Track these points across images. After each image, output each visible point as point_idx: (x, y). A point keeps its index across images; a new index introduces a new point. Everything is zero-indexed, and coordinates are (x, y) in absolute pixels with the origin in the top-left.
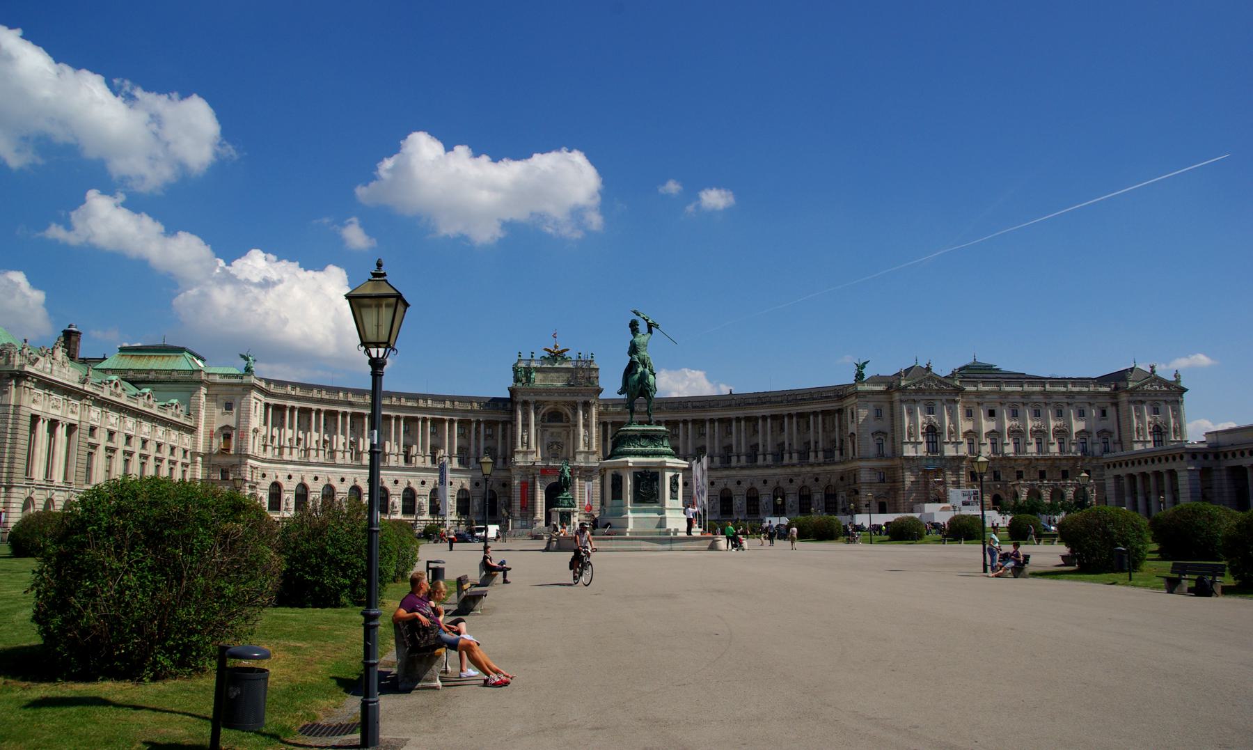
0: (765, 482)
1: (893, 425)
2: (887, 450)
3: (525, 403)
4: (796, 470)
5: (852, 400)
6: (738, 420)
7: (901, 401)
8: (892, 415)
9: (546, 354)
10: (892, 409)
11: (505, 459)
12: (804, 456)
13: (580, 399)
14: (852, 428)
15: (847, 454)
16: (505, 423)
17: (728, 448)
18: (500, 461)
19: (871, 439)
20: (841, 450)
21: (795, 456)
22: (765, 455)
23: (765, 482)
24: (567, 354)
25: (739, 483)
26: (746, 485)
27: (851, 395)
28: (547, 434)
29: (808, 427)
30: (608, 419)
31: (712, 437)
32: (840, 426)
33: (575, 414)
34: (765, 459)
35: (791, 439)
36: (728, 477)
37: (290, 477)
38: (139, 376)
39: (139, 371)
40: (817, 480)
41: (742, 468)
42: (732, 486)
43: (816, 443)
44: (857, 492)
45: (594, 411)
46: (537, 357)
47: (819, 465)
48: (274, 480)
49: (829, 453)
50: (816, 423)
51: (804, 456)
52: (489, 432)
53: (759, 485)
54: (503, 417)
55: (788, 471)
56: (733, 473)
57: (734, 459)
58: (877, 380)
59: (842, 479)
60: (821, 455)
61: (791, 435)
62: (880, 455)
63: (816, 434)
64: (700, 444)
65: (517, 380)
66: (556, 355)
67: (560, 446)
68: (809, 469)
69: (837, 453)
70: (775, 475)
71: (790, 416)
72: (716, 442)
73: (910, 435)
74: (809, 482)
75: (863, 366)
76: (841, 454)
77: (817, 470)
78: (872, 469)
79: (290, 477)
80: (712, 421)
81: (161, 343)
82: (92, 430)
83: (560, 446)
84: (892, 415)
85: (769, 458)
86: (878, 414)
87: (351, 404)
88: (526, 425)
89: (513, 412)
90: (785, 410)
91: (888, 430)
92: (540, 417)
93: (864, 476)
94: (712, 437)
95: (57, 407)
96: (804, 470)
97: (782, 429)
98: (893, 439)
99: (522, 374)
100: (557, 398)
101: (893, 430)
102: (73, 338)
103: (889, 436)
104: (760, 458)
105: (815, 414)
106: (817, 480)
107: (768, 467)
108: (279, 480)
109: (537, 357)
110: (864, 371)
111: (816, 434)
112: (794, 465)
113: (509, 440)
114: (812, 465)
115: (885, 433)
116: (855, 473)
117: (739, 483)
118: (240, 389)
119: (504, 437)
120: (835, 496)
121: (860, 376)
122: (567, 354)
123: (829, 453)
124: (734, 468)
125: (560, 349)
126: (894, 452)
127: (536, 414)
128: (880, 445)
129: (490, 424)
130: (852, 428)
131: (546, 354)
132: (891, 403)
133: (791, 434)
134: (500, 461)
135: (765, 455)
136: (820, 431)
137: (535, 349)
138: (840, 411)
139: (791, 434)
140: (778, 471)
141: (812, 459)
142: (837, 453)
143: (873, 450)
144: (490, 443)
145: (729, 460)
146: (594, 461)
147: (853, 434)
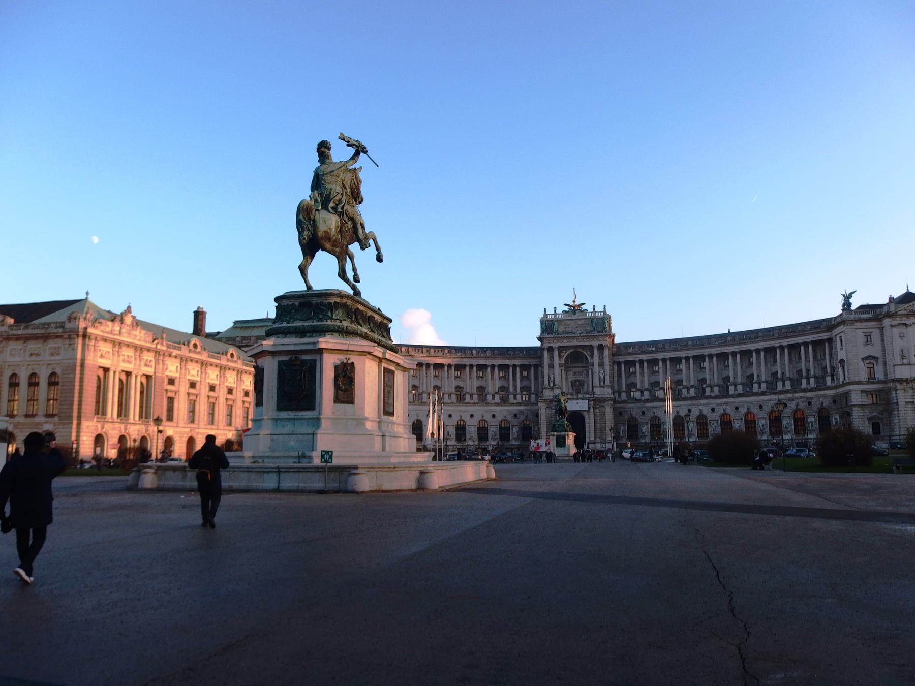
0: (761, 407)
1: (884, 349)
2: (879, 375)
3: (551, 349)
4: (790, 395)
5: (841, 328)
6: (734, 354)
7: (892, 326)
8: (883, 341)
9: (566, 308)
10: (882, 335)
11: (537, 395)
12: (796, 383)
13: (595, 343)
14: (841, 355)
15: (838, 379)
17: (727, 379)
18: (533, 397)
19: (861, 364)
20: (832, 376)
21: (788, 383)
22: (759, 383)
23: (761, 407)
24: (583, 307)
25: (737, 408)
26: (743, 410)
27: (838, 324)
28: (571, 373)
29: (800, 358)
30: (621, 359)
31: (711, 370)
32: (831, 354)
33: (592, 356)
34: (760, 387)
35: (783, 369)
36: (726, 403)
40: (810, 403)
41: (740, 395)
42: (730, 410)
43: (808, 371)
44: (849, 414)
45: (607, 352)
46: (559, 311)
47: (811, 390)
49: (820, 379)
50: (807, 352)
51: (796, 383)
52: (525, 373)
53: (755, 410)
54: (534, 362)
56: (731, 400)
57: (732, 388)
58: (864, 308)
59: (834, 402)
60: (812, 381)
61: (783, 365)
62: (872, 379)
63: (807, 363)
64: (701, 376)
65: (543, 331)
66: (574, 309)
67: (582, 383)
68: (802, 394)
69: (828, 379)
70: (770, 400)
71: (782, 348)
72: (715, 374)
73: (903, 357)
74: (802, 405)
75: (850, 296)
76: (833, 380)
77: (809, 394)
78: (863, 392)
80: (710, 356)
81: (265, 317)
82: (171, 381)
83: (582, 383)
84: (883, 341)
85: (764, 385)
86: (868, 340)
88: (551, 366)
89: (541, 357)
90: (777, 343)
91: (878, 354)
92: (563, 361)
93: (856, 398)
94: (711, 370)
95: (130, 362)
96: (797, 395)
97: (775, 361)
98: (885, 364)
99: (548, 326)
100: (575, 343)
101: (884, 355)
102: (200, 317)
103: (881, 360)
104: (756, 386)
105: (806, 344)
106: (810, 403)
107: (763, 394)
109: (559, 311)
110: (851, 300)
111: (807, 363)
112: (787, 392)
113: (540, 379)
114: (805, 391)
115: (876, 358)
116: (846, 395)
117: (737, 408)
119: (536, 378)
120: (828, 418)
121: (847, 305)
122: (583, 307)
123: (820, 379)
124: (732, 396)
125: (577, 303)
126: (886, 374)
127: (560, 357)
128: (871, 369)
129: (524, 367)
130: (841, 355)
131: (566, 308)
132: (882, 329)
133: (783, 364)
134: (533, 397)
135: (759, 383)
136: (811, 359)
137: (557, 305)
138: (830, 341)
139: (783, 364)
141: (804, 384)
142: (828, 379)
143: (863, 375)
144: (525, 383)
145: (728, 390)
146: (607, 392)
147: (842, 361)
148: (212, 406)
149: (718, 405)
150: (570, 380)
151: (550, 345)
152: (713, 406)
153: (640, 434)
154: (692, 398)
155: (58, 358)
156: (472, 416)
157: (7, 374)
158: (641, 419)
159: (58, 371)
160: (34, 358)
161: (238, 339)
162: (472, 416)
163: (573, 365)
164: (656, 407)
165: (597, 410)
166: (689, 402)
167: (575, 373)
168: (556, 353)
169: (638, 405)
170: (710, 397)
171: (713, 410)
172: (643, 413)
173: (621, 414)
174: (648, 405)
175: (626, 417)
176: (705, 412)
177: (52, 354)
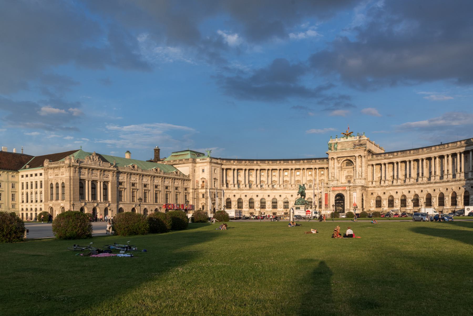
16: (327, 168)
25: (434, 190)
36: (429, 187)
37: (234, 196)
38: (175, 163)
39: (175, 161)
48: (228, 197)
55: (458, 183)
56: (431, 185)
79: (234, 196)
83: (351, 177)
87: (259, 166)
108: (230, 197)
117: (434, 190)
118: (205, 164)
140: (453, 183)
148: (94, 196)
149: (424, 188)
150: (345, 175)
151: (332, 157)
152: (422, 189)
153: (382, 205)
154: (412, 185)
155: (64, 176)
156: (292, 196)
157: (50, 183)
158: (383, 197)
159: (64, 182)
160: (57, 177)
161: (172, 161)
162: (292, 196)
163: (348, 167)
164: (391, 190)
165: (352, 192)
166: (409, 187)
167: (348, 171)
168: (336, 161)
169: (382, 188)
170: (421, 184)
171: (422, 191)
172: (384, 193)
173: (372, 194)
174: (387, 188)
175: (375, 196)
176: (417, 193)
177: (62, 175)
